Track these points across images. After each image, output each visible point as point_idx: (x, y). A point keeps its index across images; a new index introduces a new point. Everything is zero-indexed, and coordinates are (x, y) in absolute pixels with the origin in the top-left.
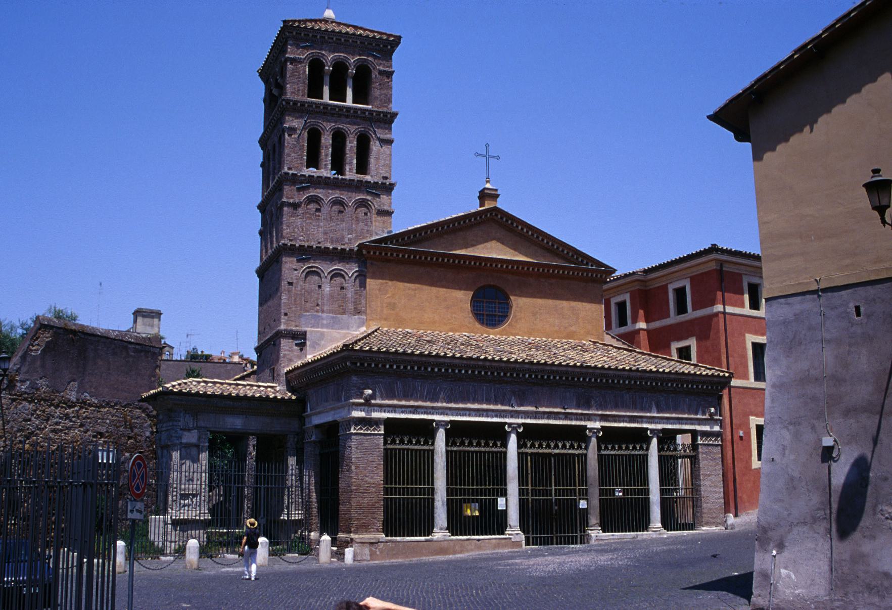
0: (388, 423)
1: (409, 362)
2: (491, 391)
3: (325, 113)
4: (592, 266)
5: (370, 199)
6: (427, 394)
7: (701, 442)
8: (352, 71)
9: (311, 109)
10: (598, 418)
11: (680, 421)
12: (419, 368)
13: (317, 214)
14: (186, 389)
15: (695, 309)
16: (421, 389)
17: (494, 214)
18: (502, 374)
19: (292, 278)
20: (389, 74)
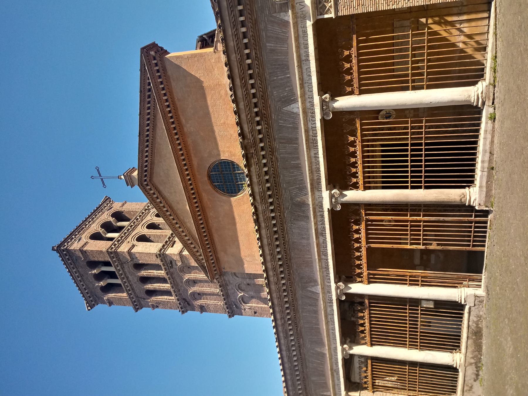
2: (306, 309)
3: (133, 289)
6: (319, 360)
7: (332, 10)
10: (317, 193)
11: (304, 58)
17: (146, 183)
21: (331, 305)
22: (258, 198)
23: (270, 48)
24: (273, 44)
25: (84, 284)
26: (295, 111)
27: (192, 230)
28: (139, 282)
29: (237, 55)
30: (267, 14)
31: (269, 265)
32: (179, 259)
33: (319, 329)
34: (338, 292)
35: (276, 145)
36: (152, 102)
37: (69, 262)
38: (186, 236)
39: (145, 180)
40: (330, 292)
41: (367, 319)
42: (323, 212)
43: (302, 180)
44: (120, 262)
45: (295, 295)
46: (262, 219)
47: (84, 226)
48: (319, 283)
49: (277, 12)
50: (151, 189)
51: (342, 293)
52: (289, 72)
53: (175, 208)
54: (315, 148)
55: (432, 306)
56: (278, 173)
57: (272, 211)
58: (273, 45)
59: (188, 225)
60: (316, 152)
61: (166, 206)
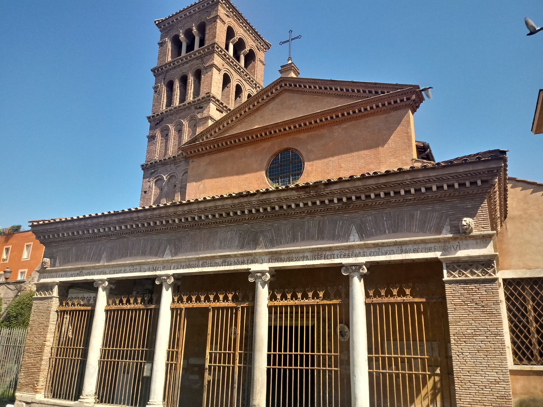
2: (148, 243)
6: (93, 255)
7: (451, 278)
10: (266, 258)
11: (404, 248)
16: (89, 251)
17: (283, 85)
21: (151, 269)
22: (264, 197)
23: (416, 214)
24: (420, 217)
25: (182, 19)
26: (350, 237)
27: (233, 130)
28: (182, 75)
29: (409, 181)
30: (449, 213)
31: (195, 207)
32: (204, 116)
33: (126, 256)
34: (164, 277)
35: (318, 217)
36: (364, 95)
37: (206, 5)
38: (228, 124)
39: (286, 85)
40: (164, 268)
41: (134, 307)
42: (248, 263)
43: (281, 243)
44: (203, 56)
45: (163, 233)
46: (242, 201)
47: (241, 21)
48: (174, 258)
49: (451, 222)
50: (276, 90)
51: (162, 281)
52: (390, 233)
53: (256, 114)
54: (313, 256)
55: (145, 375)
56: (288, 218)
57: (250, 211)
58: (418, 217)
59: (239, 127)
60: (309, 257)
61: (259, 105)
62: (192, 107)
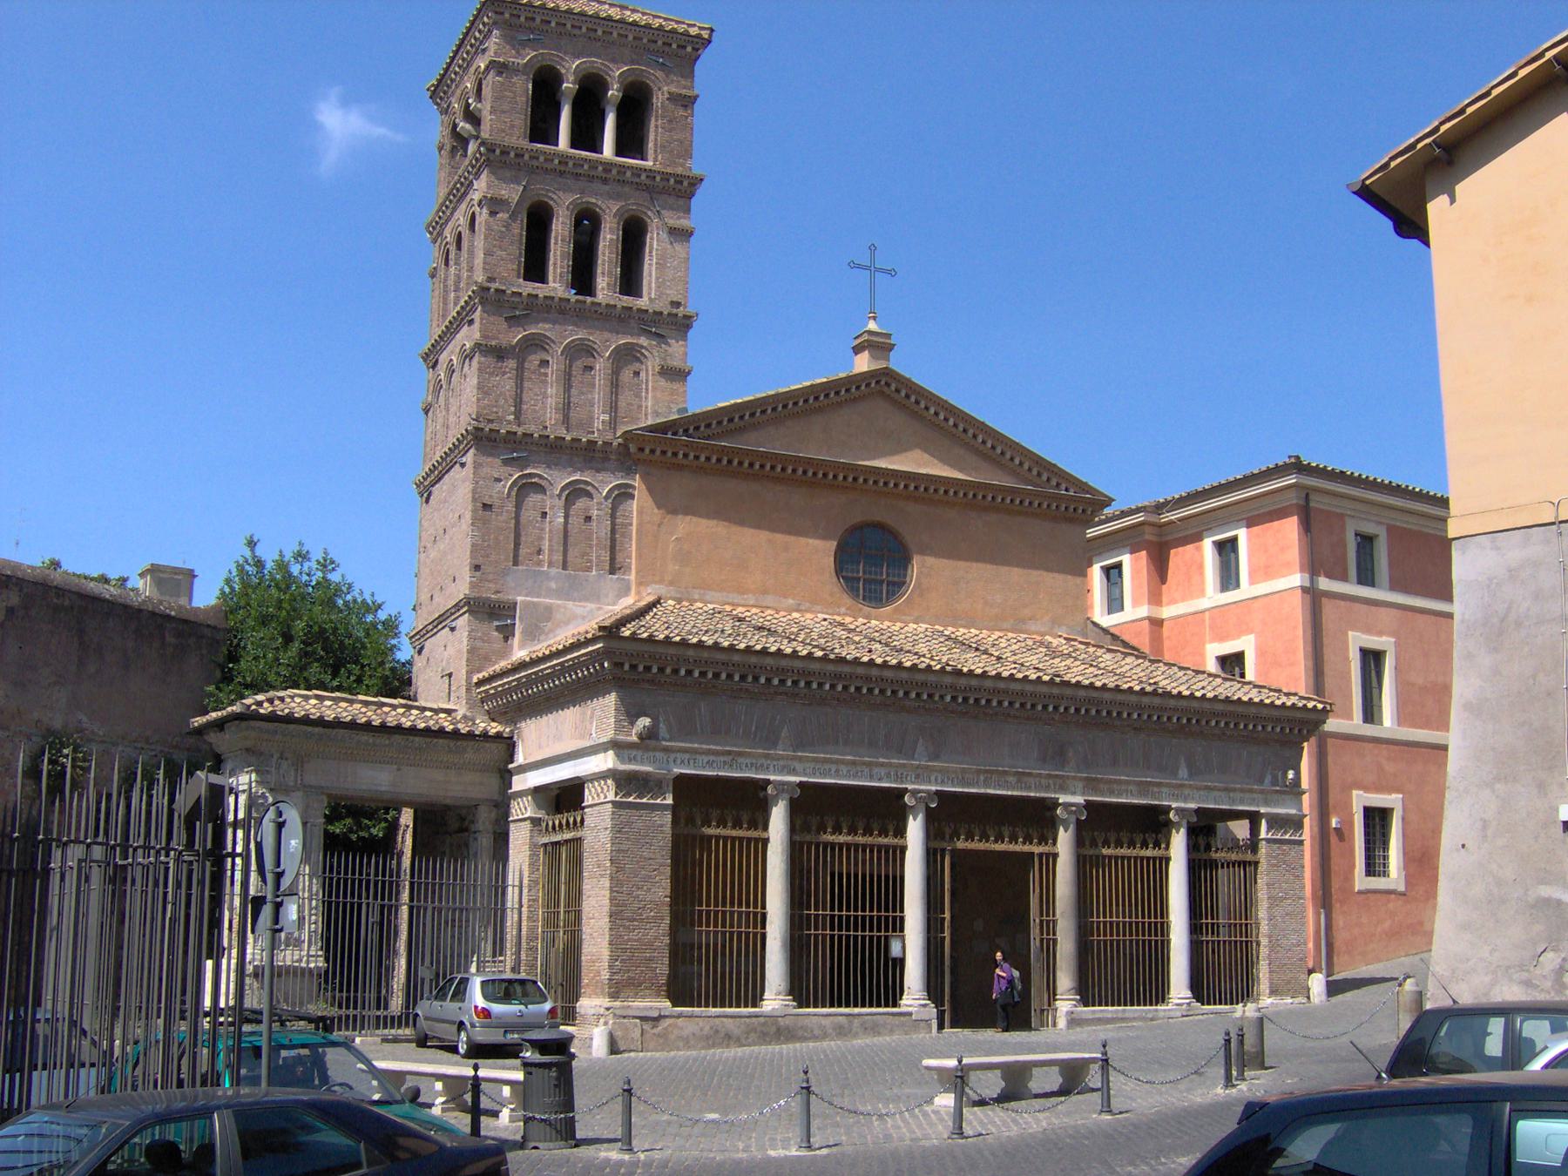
0: (684, 786)
1: (723, 664)
3: (562, 173)
4: (1067, 490)
5: (645, 344)
8: (614, 93)
9: (535, 163)
12: (743, 678)
13: (542, 370)
14: (283, 711)
15: (1253, 581)
17: (883, 383)
18: (901, 694)
19: (491, 496)
20: (688, 102)
62: (632, 321)
